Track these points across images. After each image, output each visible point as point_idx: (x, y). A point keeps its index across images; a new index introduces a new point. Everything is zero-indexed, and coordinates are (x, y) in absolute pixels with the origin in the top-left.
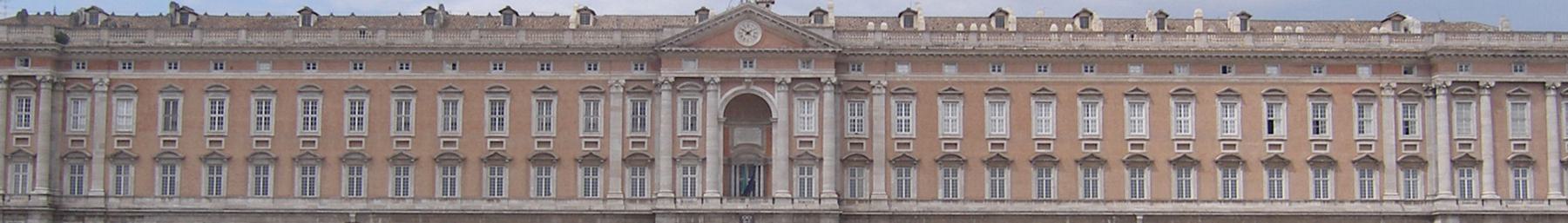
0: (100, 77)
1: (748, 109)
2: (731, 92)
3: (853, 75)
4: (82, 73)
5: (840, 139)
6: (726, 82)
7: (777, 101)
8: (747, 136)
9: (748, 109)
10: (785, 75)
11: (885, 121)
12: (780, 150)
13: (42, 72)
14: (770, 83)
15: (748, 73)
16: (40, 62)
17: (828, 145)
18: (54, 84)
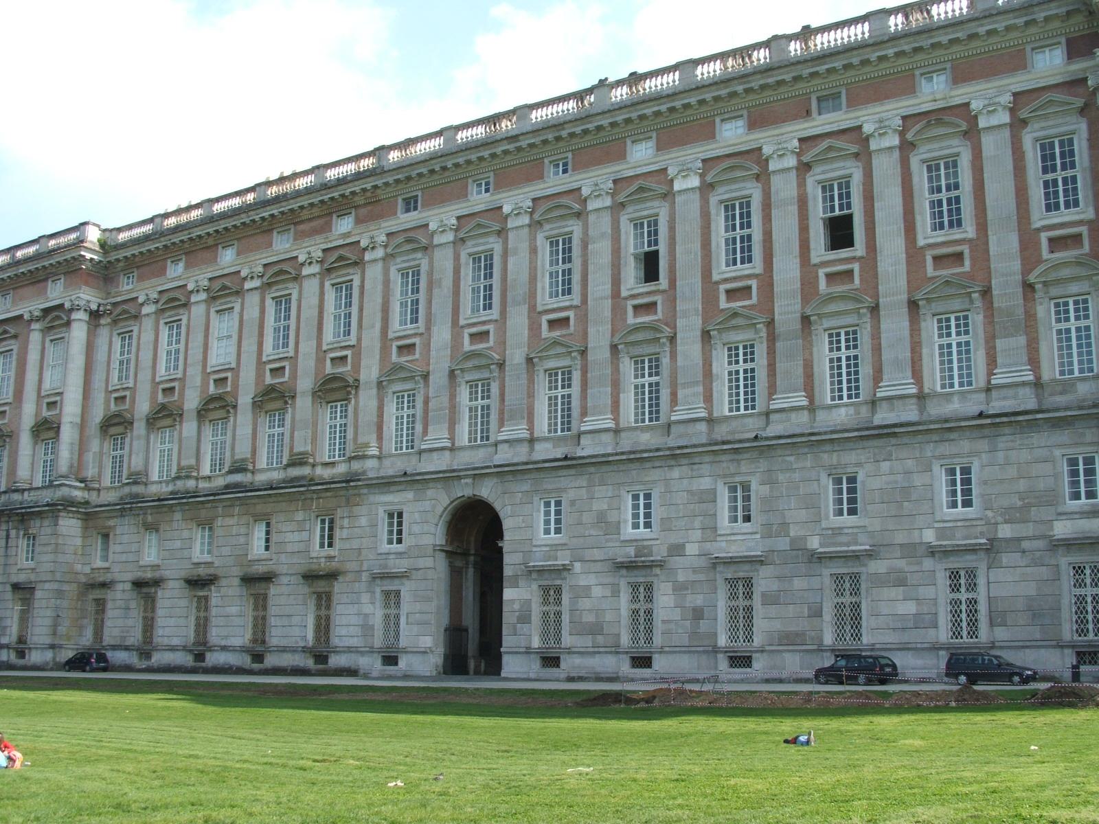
18: (95, 315)
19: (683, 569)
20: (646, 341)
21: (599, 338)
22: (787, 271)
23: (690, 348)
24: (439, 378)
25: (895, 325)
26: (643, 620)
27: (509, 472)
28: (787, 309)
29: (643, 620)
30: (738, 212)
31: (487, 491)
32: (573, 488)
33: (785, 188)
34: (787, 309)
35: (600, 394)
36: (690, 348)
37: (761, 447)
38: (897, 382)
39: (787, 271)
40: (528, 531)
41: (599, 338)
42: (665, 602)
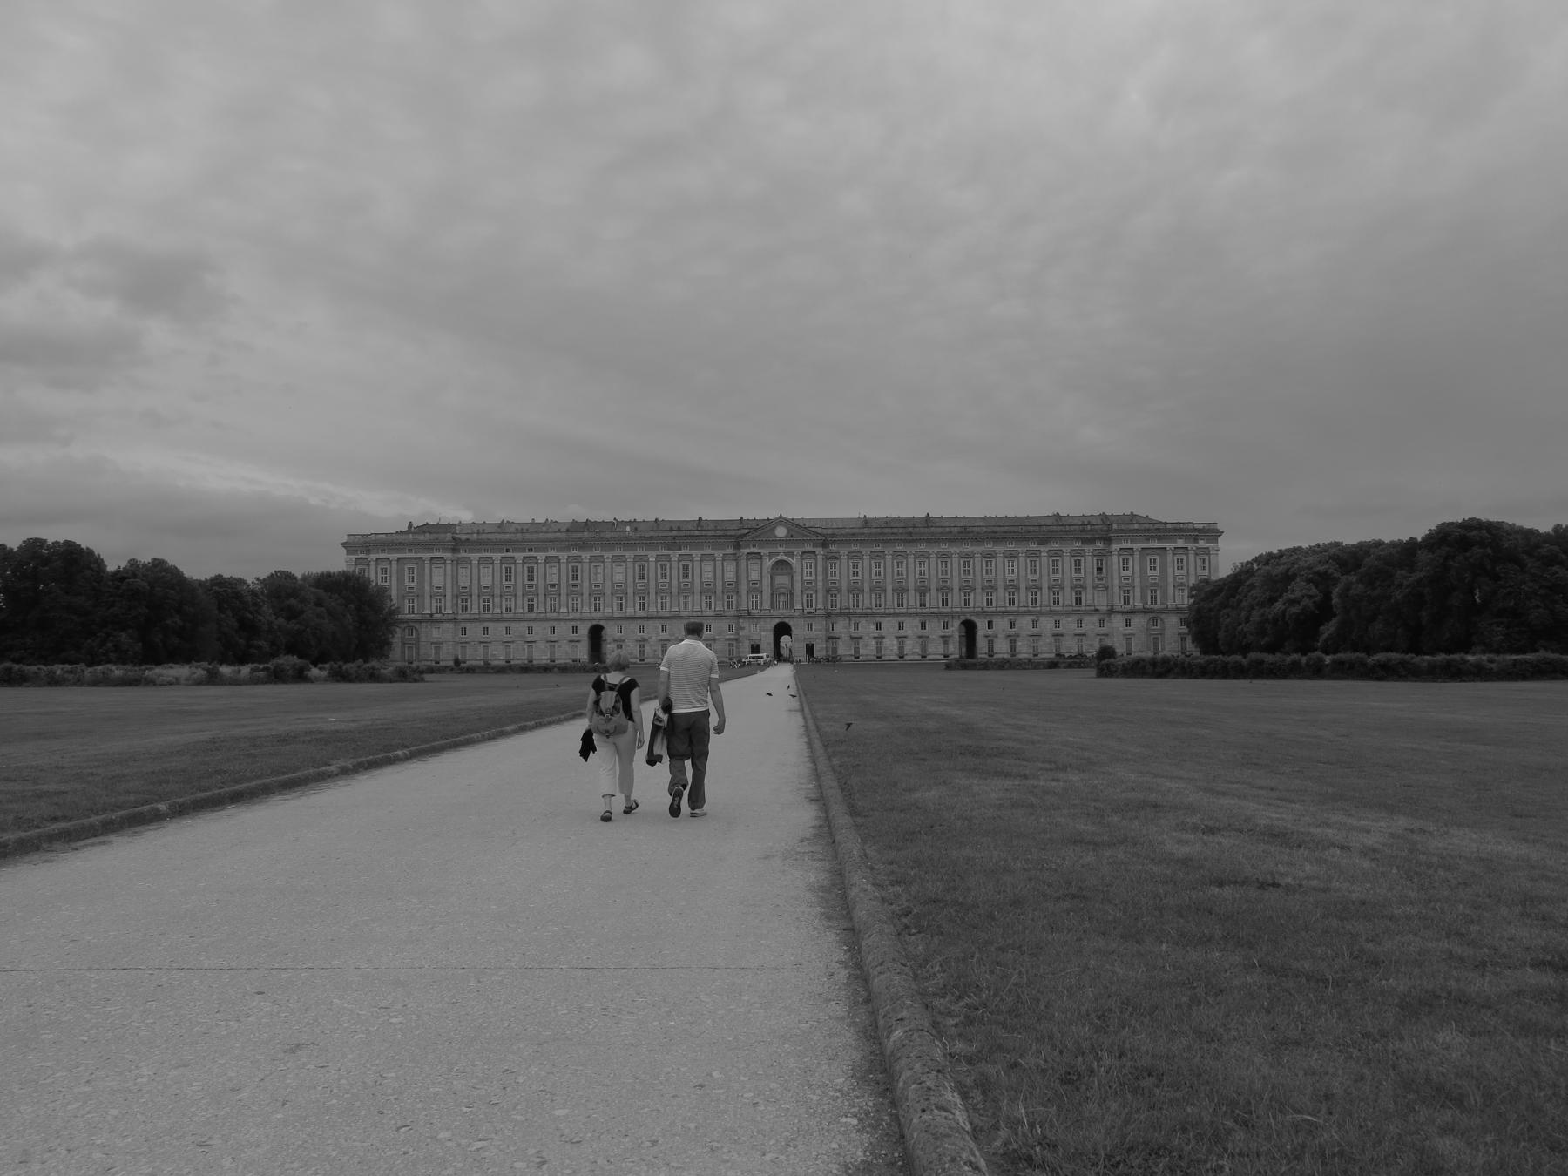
0: (475, 557)
1: (782, 565)
2: (775, 559)
3: (833, 548)
4: (463, 555)
5: (825, 579)
6: (771, 555)
7: (795, 562)
8: (782, 580)
9: (782, 565)
10: (798, 551)
11: (843, 573)
12: (798, 586)
13: (448, 555)
14: (792, 555)
15: (781, 549)
16: (445, 550)
17: (820, 584)
19: (652, 641)
20: (642, 595)
21: (630, 591)
22: (675, 582)
23: (652, 595)
24: (586, 595)
25: (697, 597)
26: (642, 652)
27: (607, 619)
28: (675, 590)
29: (642, 652)
30: (664, 568)
31: (602, 623)
32: (624, 624)
33: (675, 565)
34: (675, 590)
35: (630, 603)
36: (652, 595)
37: (670, 618)
38: (697, 608)
39: (675, 582)
40: (610, 632)
41: (630, 591)
42: (647, 648)
